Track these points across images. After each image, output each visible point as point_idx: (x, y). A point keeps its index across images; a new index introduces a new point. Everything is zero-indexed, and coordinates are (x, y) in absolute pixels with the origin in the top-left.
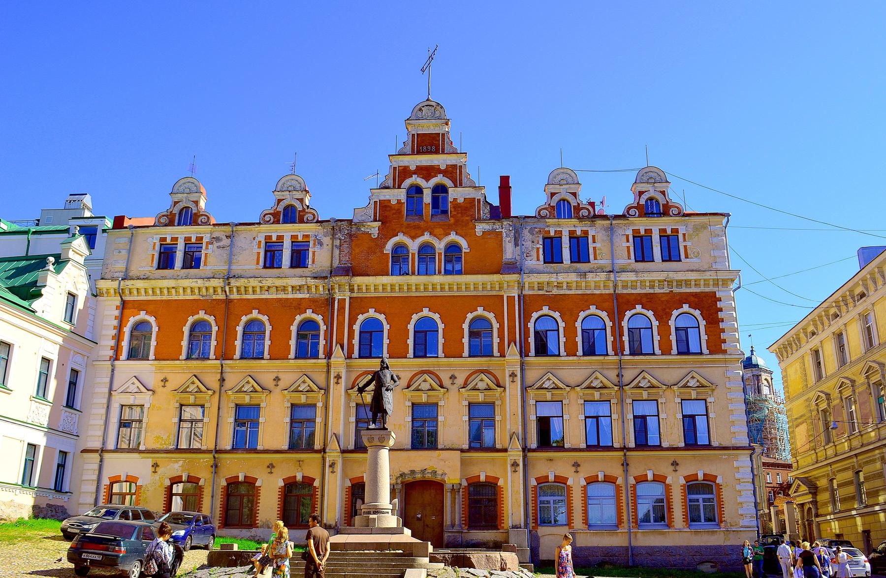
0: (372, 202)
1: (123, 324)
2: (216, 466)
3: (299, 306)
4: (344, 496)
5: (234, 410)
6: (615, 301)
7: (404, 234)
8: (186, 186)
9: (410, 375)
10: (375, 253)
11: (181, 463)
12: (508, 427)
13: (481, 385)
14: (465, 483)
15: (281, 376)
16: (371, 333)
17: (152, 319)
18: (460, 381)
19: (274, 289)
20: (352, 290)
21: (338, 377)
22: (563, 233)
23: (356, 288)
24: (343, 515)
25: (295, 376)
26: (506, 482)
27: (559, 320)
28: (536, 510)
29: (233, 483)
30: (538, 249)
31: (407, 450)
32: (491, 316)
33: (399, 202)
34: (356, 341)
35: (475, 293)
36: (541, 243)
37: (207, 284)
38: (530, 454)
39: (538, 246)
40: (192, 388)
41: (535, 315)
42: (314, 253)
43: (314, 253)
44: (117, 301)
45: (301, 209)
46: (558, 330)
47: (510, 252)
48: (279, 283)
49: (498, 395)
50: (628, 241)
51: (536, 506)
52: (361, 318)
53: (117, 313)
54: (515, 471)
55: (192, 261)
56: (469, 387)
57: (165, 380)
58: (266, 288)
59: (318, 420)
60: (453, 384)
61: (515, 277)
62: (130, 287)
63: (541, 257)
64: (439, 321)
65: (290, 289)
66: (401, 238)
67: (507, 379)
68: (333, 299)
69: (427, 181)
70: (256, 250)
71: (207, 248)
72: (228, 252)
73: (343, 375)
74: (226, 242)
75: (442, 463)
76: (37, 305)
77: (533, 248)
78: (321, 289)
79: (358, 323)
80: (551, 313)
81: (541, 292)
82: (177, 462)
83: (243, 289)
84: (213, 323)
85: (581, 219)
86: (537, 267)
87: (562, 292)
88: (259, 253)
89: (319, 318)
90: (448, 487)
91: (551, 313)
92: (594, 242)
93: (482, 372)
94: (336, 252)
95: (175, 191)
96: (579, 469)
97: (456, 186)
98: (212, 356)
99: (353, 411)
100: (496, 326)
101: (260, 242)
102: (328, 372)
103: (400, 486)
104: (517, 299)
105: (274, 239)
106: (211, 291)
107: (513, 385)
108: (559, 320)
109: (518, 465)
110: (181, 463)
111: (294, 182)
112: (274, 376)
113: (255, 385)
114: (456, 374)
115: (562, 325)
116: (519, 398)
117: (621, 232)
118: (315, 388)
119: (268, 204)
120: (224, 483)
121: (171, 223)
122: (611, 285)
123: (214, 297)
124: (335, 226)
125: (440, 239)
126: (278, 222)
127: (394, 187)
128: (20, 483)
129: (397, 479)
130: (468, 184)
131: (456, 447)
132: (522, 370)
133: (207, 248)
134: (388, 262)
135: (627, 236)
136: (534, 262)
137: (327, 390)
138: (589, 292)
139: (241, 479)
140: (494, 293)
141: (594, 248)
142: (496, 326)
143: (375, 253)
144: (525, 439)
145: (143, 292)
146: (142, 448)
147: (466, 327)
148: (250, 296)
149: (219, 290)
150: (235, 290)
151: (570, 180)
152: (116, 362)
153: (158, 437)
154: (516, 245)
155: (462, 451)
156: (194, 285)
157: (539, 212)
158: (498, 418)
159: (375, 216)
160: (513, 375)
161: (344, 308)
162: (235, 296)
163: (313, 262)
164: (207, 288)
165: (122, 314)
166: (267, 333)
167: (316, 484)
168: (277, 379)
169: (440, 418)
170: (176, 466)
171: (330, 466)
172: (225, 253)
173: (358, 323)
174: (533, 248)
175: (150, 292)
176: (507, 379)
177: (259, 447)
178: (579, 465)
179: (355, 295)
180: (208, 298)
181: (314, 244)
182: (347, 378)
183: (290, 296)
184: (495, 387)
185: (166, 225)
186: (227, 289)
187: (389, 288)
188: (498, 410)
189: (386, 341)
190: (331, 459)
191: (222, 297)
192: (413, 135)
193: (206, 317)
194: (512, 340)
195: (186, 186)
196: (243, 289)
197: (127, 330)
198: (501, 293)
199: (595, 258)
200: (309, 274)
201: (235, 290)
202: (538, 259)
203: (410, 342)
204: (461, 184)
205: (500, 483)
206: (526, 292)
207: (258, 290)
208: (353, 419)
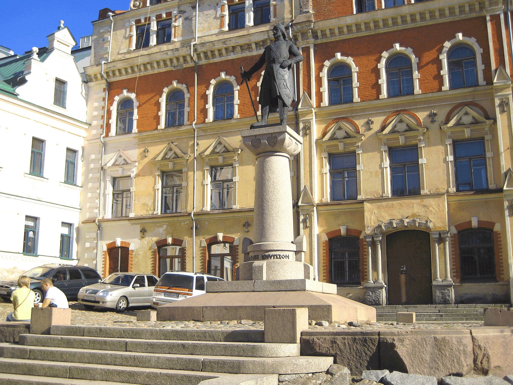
11: (165, 227)
14: (454, 231)
17: (133, 96)
19: (238, 49)
20: (316, 37)
23: (319, 34)
31: (387, 199)
32: (472, 41)
35: (451, 19)
37: (176, 54)
40: (170, 155)
44: (104, 86)
48: (242, 42)
49: (487, 129)
52: (327, 63)
55: (164, 36)
57: (146, 151)
58: (231, 49)
60: (433, 122)
62: (112, 69)
65: (254, 46)
76: (19, 90)
79: (325, 70)
82: (161, 226)
83: (209, 54)
88: (223, 17)
99: (326, 162)
100: (479, 51)
106: (181, 60)
110: (165, 227)
120: (204, 244)
123: (185, 66)
128: (22, 252)
139: (221, 238)
140: (474, 15)
142: (479, 51)
145: (123, 72)
146: (132, 215)
148: (217, 60)
150: (202, 55)
152: (107, 139)
153: (144, 205)
156: (165, 57)
158: (489, 154)
162: (203, 62)
164: (178, 59)
170: (161, 230)
171: (304, 221)
173: (325, 70)
175: (130, 71)
176: (498, 110)
179: (319, 41)
180: (179, 68)
184: (482, 119)
187: (354, 28)
188: (488, 146)
189: (355, 83)
191: (191, 64)
193: (180, 86)
196: (209, 54)
197: (114, 108)
201: (202, 55)
205: (497, 228)
207: (224, 52)
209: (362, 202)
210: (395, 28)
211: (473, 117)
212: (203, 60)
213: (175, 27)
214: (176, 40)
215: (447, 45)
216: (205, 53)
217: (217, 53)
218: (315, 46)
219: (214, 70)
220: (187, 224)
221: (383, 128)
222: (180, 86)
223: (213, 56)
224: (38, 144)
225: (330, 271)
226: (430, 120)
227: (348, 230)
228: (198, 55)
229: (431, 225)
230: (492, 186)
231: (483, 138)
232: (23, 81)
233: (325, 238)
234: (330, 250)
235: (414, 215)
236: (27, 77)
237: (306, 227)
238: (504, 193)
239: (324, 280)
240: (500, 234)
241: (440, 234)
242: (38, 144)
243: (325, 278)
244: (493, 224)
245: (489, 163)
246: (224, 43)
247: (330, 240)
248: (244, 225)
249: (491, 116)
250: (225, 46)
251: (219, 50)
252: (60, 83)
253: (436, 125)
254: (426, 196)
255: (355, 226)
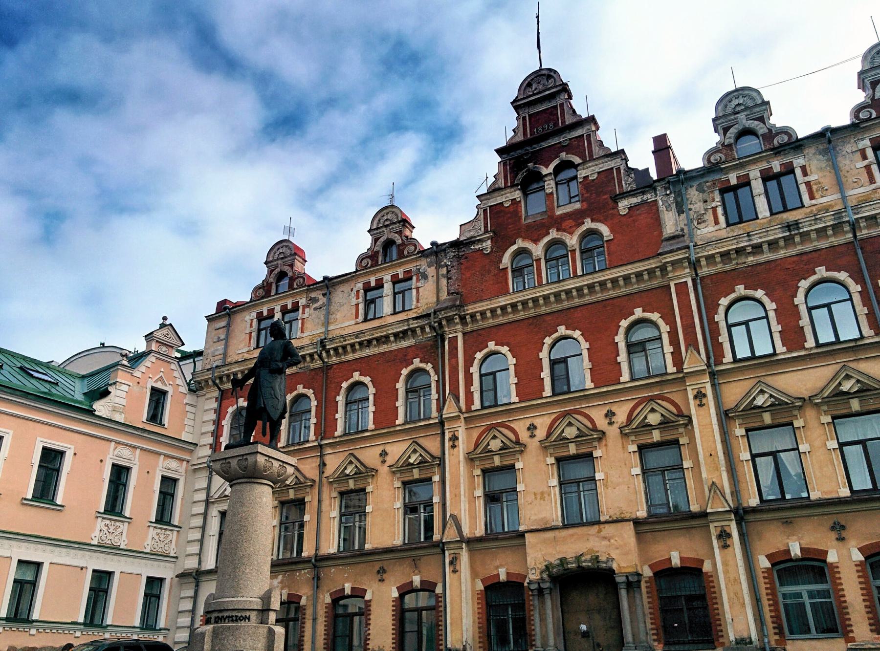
0: (481, 212)
1: (222, 415)
2: (318, 578)
3: (404, 357)
4: (476, 606)
5: (337, 501)
6: (859, 251)
7: (524, 239)
8: (281, 251)
9: (548, 420)
10: (489, 272)
11: (280, 577)
12: (704, 475)
13: (654, 419)
14: (647, 572)
15: (388, 448)
16: (494, 374)
18: (621, 416)
19: (375, 342)
21: (454, 438)
22: (751, 176)
23: (468, 319)
24: (477, 635)
25: (403, 446)
26: (714, 565)
27: (766, 300)
28: (777, 610)
29: (338, 598)
30: (714, 209)
33: (513, 200)
34: (475, 387)
36: (718, 198)
38: (751, 517)
39: (714, 204)
41: (724, 302)
42: (418, 289)
43: (418, 289)
44: (216, 393)
45: (400, 241)
46: (767, 317)
47: (671, 222)
50: (865, 157)
51: (775, 604)
52: (479, 356)
53: (215, 405)
54: (725, 546)
56: (635, 424)
59: (436, 499)
61: (680, 255)
63: (722, 219)
64: (581, 339)
65: (392, 338)
66: (520, 243)
67: (692, 402)
68: (443, 341)
69: (547, 167)
70: (354, 301)
71: (303, 313)
72: (324, 312)
73: (461, 434)
74: (323, 300)
75: (605, 542)
77: (706, 210)
78: (428, 330)
79: (476, 363)
80: (750, 292)
81: (728, 267)
83: (340, 350)
84: (312, 397)
85: (778, 151)
86: (715, 234)
87: (761, 258)
88: (357, 305)
89: (429, 367)
90: (620, 579)
91: (750, 292)
92: (805, 174)
93: (651, 399)
94: (444, 282)
95: (271, 259)
96: (844, 534)
97: (585, 162)
98: (312, 437)
100: (665, 328)
101: (358, 292)
102: (443, 434)
103: (548, 585)
104: (690, 284)
105: (373, 284)
107: (702, 410)
108: (766, 300)
109: (729, 536)
111: (389, 216)
112: (379, 450)
113: (358, 465)
114: (614, 409)
115: (771, 306)
116: (716, 428)
117: (849, 148)
118: (428, 458)
119: (365, 243)
120: (328, 600)
121: (268, 294)
122: (847, 228)
123: (312, 366)
124: (437, 250)
125: (571, 233)
126: (376, 264)
127: (506, 187)
129: (542, 573)
130: (602, 153)
131: (628, 516)
132: (713, 385)
133: (303, 313)
134: (507, 279)
135: (863, 153)
136: (711, 228)
137: (442, 460)
138: (808, 247)
139: (348, 591)
140: (655, 283)
141: (808, 184)
143: (489, 272)
144: (736, 493)
147: (620, 339)
148: (350, 357)
149: (316, 357)
150: (332, 352)
151: (750, 103)
154: (680, 211)
155: (637, 522)
157: (709, 161)
158: (686, 464)
159: (486, 226)
160: (700, 396)
161: (457, 349)
162: (334, 360)
163: (418, 301)
165: (220, 406)
166: (371, 398)
167: (439, 590)
168: (384, 454)
169: (598, 476)
171: (451, 563)
172: (321, 314)
174: (706, 210)
176: (692, 402)
177: (367, 546)
178: (843, 527)
179: (469, 328)
181: (418, 280)
182: (469, 436)
183: (394, 347)
185: (263, 298)
186: (324, 355)
188: (685, 451)
190: (452, 552)
191: (318, 364)
192: (524, 118)
194: (692, 342)
195: (281, 251)
196: (340, 350)
197: (226, 423)
198: (665, 283)
199: (812, 197)
200: (414, 315)
201: (332, 352)
202: (717, 222)
203: (546, 374)
204: (591, 155)
205: (707, 567)
206: (704, 271)
207: (357, 347)
208: (479, 492)
209: (521, 535)
210: (559, 307)
211: (662, 415)
212: (334, 358)
213: (303, 319)
214: (302, 335)
215: (624, 323)
216: (336, 349)
217: (349, 348)
218: (464, 334)
219: (349, 367)
220: (308, 573)
221: (549, 435)
222: (305, 391)
223: (345, 352)
224: (120, 474)
225: (489, 636)
226: (607, 421)
227: (508, 574)
228: (328, 352)
229: (615, 566)
230: (695, 508)
231: (676, 442)
232: (106, 393)
233: (480, 586)
234: (487, 604)
235: (590, 551)
236: (110, 389)
237: (455, 571)
238: (710, 518)
239: (480, 647)
240: (712, 576)
241: (627, 577)
242: (120, 474)
243: (481, 645)
244: (702, 561)
245: (688, 475)
246: (357, 337)
247: (487, 588)
248: (378, 572)
249: (685, 413)
250: (358, 340)
251: (352, 345)
252: (158, 397)
253: (615, 427)
254: (606, 522)
255: (516, 569)
